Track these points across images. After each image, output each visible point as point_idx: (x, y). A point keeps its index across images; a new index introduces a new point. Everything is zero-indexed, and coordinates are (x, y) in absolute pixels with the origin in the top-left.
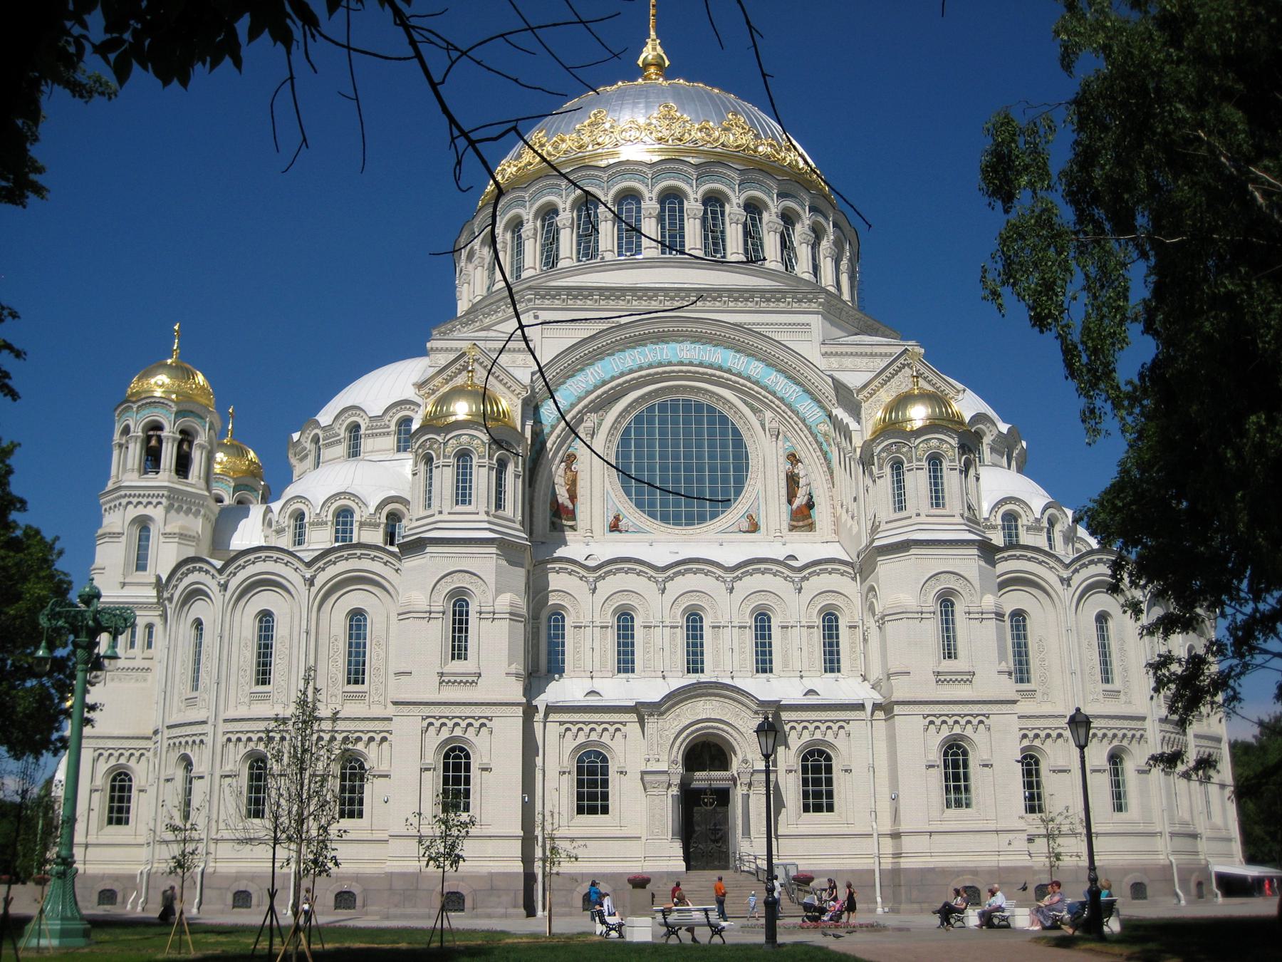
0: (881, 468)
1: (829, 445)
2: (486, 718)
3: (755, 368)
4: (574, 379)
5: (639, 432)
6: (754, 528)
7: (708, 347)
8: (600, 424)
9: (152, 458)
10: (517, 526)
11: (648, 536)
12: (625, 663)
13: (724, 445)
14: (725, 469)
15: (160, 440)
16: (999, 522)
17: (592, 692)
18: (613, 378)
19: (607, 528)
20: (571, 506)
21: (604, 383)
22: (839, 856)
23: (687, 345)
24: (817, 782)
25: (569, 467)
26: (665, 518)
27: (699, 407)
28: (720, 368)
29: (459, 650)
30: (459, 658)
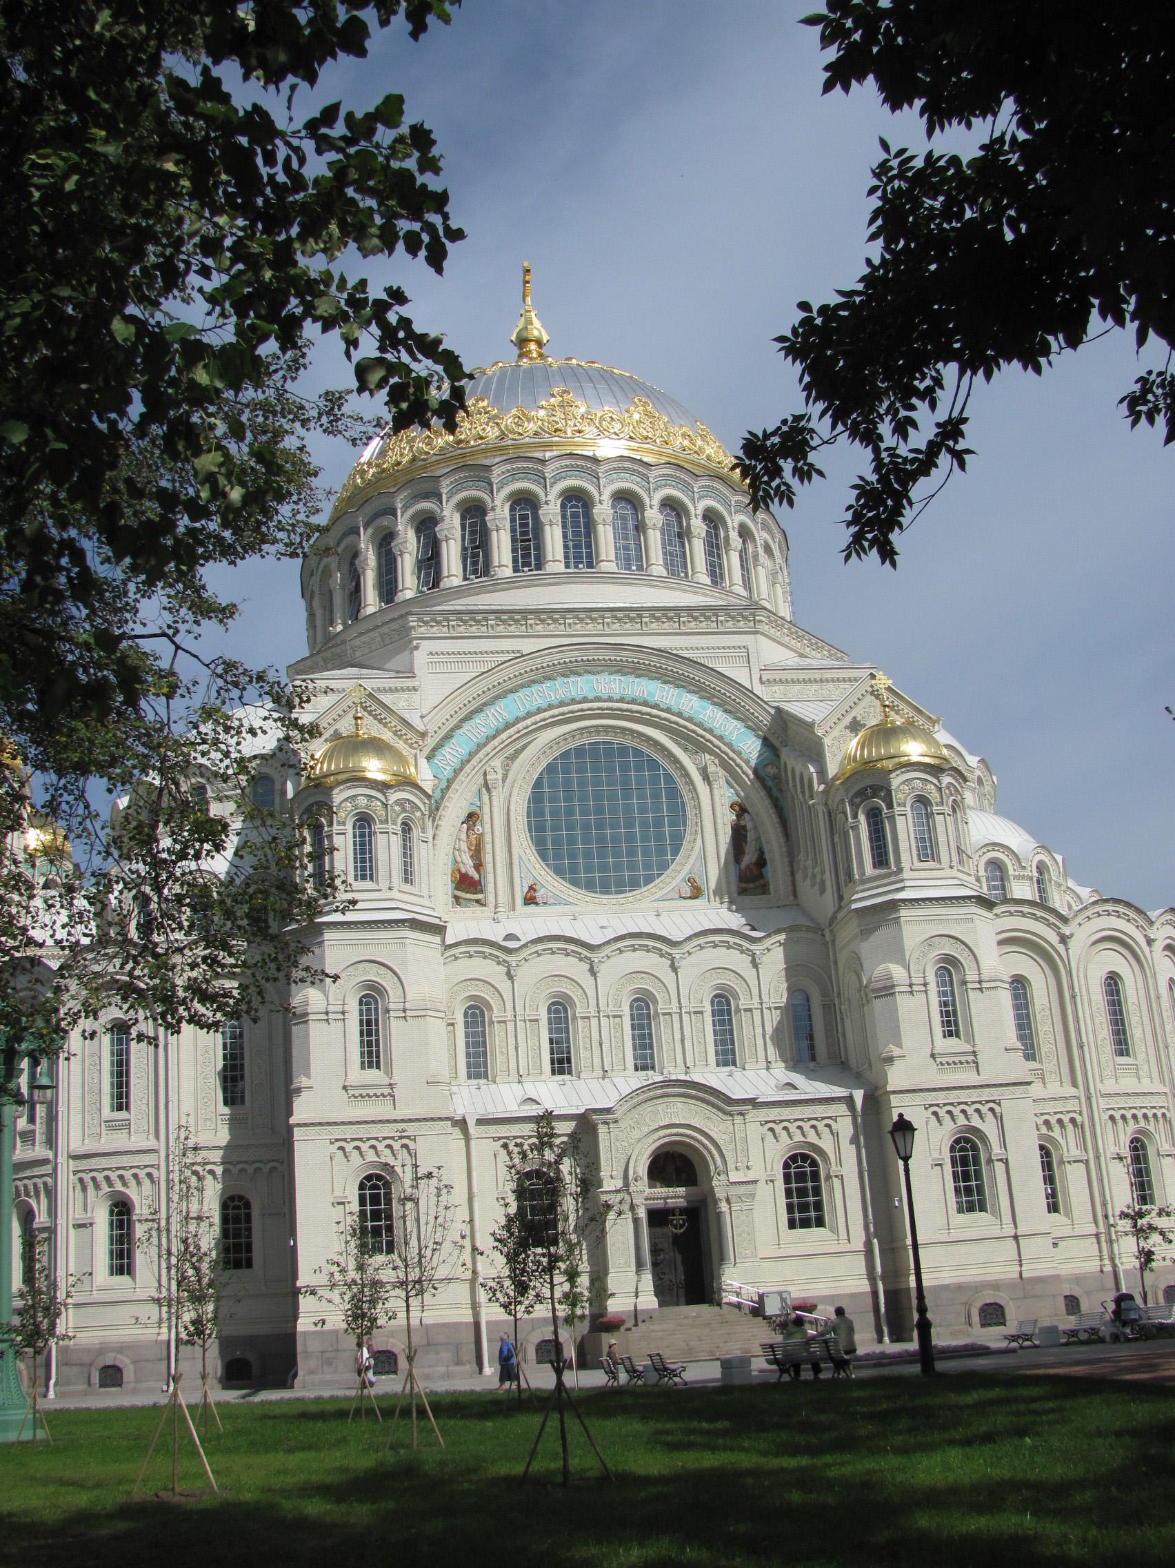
0: (855, 816)
1: (781, 790)
3: (690, 703)
6: (696, 893)
7: (631, 679)
8: (505, 777)
11: (572, 908)
12: (562, 1063)
13: (656, 795)
14: (658, 823)
16: (982, 873)
20: (476, 877)
23: (605, 677)
24: (802, 1192)
26: (590, 886)
27: (623, 750)
28: (645, 704)
29: (372, 1054)
30: (370, 1066)
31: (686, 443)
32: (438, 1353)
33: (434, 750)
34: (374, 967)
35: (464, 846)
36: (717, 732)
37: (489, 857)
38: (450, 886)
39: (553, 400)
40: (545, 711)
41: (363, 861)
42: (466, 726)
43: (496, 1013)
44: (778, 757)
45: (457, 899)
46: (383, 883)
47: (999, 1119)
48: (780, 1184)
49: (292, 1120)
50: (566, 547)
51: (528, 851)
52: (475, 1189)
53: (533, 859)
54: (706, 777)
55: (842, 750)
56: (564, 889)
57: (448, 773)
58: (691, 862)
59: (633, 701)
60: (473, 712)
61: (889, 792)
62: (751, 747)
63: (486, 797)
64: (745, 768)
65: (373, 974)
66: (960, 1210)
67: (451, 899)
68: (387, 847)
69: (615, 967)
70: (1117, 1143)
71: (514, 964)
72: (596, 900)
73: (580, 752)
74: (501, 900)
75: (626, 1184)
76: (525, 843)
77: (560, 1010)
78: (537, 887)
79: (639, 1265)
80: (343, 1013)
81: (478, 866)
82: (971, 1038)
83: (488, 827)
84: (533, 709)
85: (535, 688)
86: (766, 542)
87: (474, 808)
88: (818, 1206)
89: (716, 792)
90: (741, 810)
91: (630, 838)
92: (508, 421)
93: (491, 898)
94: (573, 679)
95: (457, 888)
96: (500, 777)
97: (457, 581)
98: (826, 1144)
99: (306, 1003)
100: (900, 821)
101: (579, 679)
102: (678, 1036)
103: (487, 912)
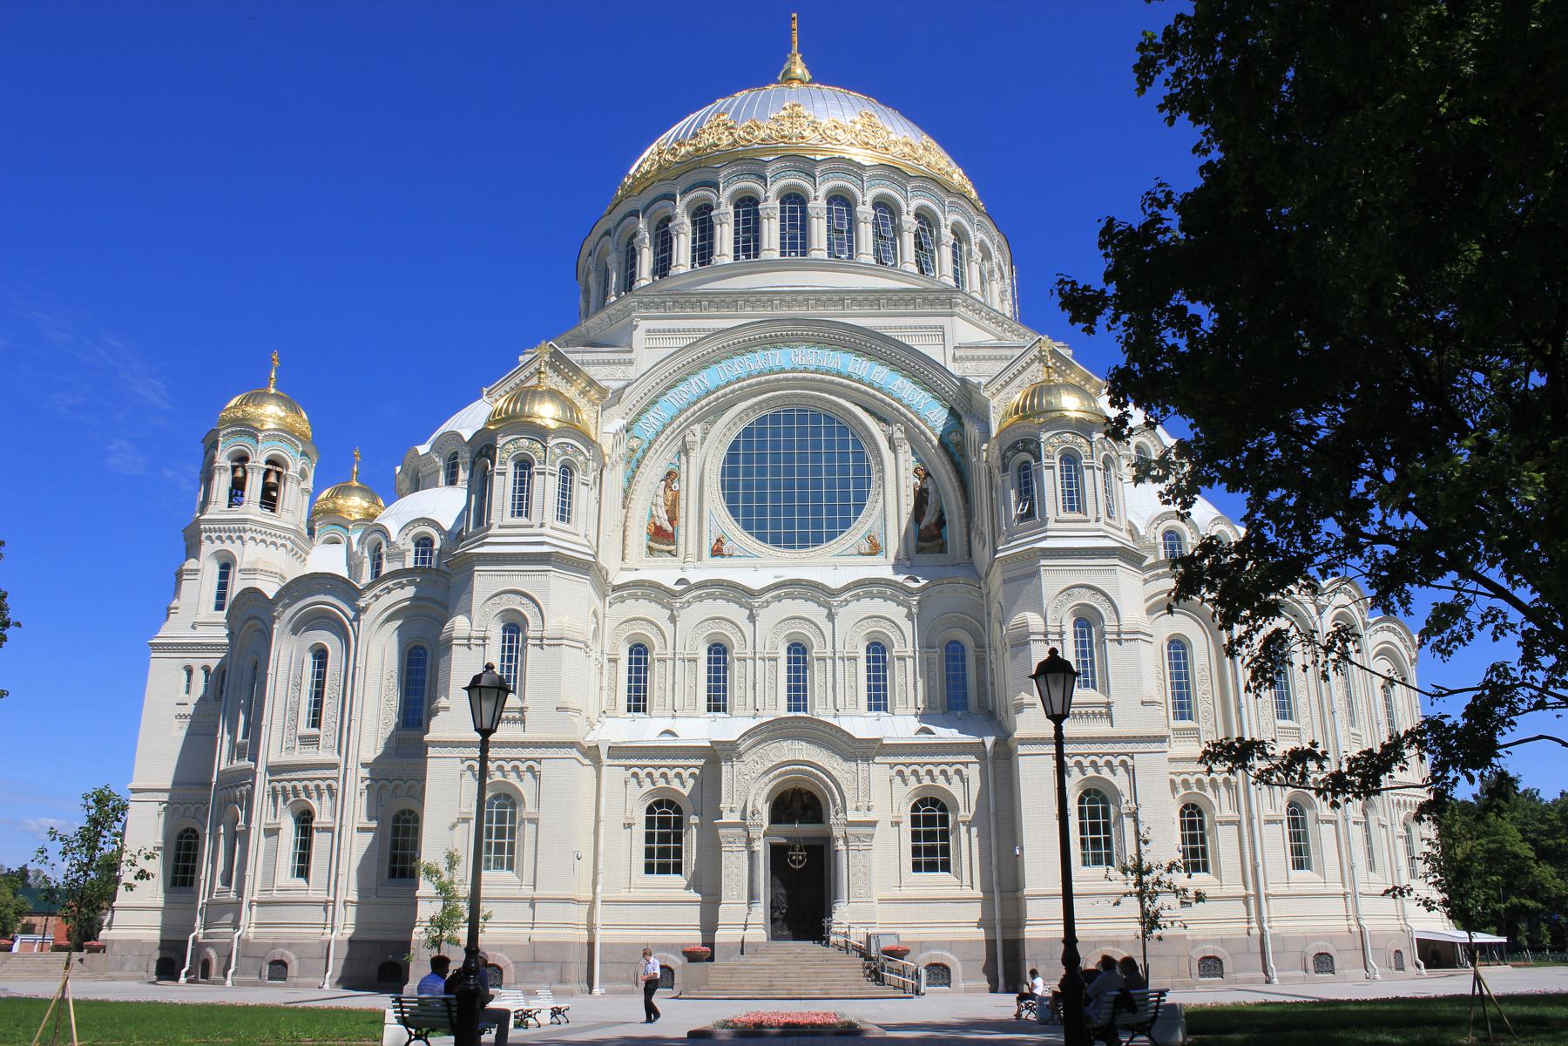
2: (534, 759)
3: (879, 374)
5: (748, 446)
6: (875, 549)
7: (827, 352)
8: (703, 439)
9: (238, 487)
11: (756, 561)
12: (717, 703)
13: (844, 457)
15: (245, 473)
16: (1160, 539)
17: (668, 732)
18: (718, 388)
19: (706, 552)
22: (955, 924)
26: (776, 541)
28: (839, 374)
31: (907, 150)
32: (542, 970)
33: (639, 414)
34: (518, 598)
35: (660, 501)
36: (906, 402)
37: (682, 512)
39: (783, 113)
41: (521, 498)
42: (671, 393)
43: (657, 650)
44: (962, 425)
46: (535, 519)
47: (1131, 772)
48: (907, 828)
49: (427, 738)
50: (782, 238)
52: (602, 814)
54: (893, 447)
55: (1001, 406)
57: (650, 435)
58: (871, 520)
59: (827, 372)
61: (1039, 445)
62: (937, 416)
63: (684, 459)
64: (929, 434)
65: (515, 603)
66: (1084, 864)
67: (645, 549)
68: (546, 488)
69: (774, 613)
70: (1273, 805)
73: (775, 418)
74: (690, 550)
75: (744, 818)
77: (719, 653)
79: (752, 897)
80: (484, 639)
81: (672, 520)
82: (1106, 690)
83: (683, 484)
86: (982, 241)
88: (946, 851)
89: (901, 457)
90: (925, 474)
91: (817, 497)
92: (739, 132)
93: (681, 549)
96: (698, 439)
97: (682, 270)
98: (956, 789)
99: (452, 629)
100: (1047, 475)
102: (830, 680)
103: (677, 561)
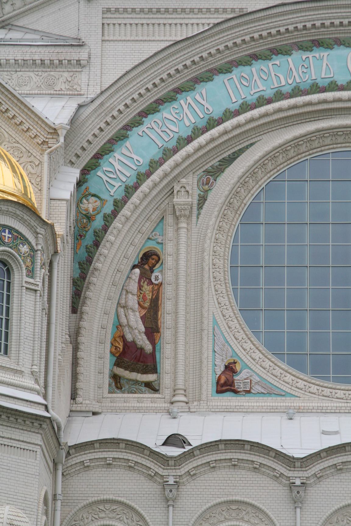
4: (157, 117)
8: (202, 200)
10: (29, 382)
19: (209, 385)
20: (148, 347)
21: (212, 123)
25: (145, 276)
26: (319, 369)
35: (133, 301)
38: (108, 361)
40: (269, 101)
42: (148, 121)
45: (117, 382)
51: (229, 313)
53: (234, 324)
56: (278, 371)
57: (116, 190)
60: (160, 102)
67: (107, 380)
71: (171, 481)
72: (327, 392)
76: (224, 301)
78: (238, 367)
84: (251, 99)
85: (258, 65)
87: (151, 245)
93: (166, 380)
94: (318, 53)
95: (118, 364)
101: (324, 53)
